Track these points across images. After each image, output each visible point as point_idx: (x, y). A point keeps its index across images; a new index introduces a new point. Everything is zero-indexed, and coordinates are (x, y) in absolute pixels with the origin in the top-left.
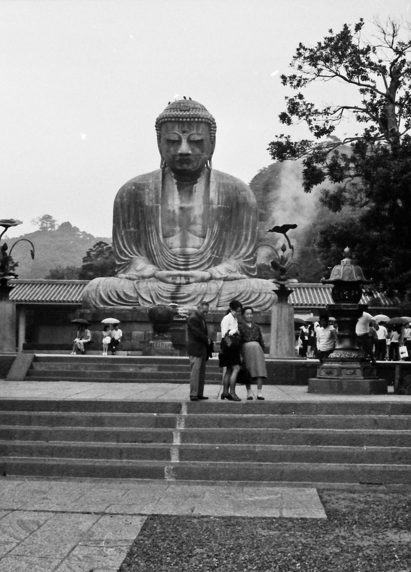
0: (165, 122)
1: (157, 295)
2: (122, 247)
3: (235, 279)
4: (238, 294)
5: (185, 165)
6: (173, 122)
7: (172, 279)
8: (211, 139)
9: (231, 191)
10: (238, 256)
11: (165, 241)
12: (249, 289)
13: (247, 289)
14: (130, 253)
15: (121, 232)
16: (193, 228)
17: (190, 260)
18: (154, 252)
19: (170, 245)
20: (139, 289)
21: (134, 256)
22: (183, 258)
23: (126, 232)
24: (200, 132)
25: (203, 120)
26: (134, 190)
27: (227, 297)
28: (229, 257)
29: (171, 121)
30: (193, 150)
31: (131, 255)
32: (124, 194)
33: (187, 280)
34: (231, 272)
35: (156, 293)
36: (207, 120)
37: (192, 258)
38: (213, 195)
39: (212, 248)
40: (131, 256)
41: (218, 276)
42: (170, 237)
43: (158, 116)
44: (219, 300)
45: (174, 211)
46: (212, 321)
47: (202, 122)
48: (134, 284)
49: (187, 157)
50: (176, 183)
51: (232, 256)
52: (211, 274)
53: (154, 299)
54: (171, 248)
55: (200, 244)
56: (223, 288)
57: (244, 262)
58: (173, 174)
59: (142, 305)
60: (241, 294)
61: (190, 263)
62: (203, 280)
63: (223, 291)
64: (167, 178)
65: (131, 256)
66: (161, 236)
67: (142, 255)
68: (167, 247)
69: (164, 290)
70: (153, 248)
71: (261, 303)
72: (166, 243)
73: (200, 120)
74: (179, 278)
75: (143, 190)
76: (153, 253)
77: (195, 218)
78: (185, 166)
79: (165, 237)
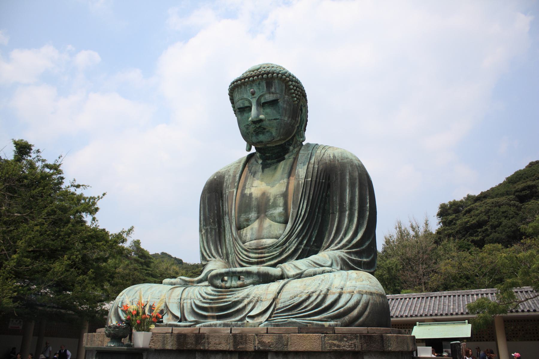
3: (315, 274)
7: (223, 280)
8: (294, 101)
10: (339, 246)
12: (323, 288)
13: (320, 288)
14: (208, 255)
22: (256, 253)
26: (215, 179)
27: (287, 303)
30: (267, 114)
31: (210, 257)
37: (268, 253)
39: (298, 236)
42: (244, 227)
44: (274, 310)
46: (232, 349)
50: (261, 164)
51: (332, 246)
54: (244, 242)
55: (281, 232)
57: (347, 253)
58: (258, 155)
60: (309, 297)
64: (253, 160)
65: (208, 259)
67: (220, 256)
69: (204, 298)
71: (342, 310)
73: (270, 75)
75: (224, 177)
77: (275, 199)
78: (261, 137)
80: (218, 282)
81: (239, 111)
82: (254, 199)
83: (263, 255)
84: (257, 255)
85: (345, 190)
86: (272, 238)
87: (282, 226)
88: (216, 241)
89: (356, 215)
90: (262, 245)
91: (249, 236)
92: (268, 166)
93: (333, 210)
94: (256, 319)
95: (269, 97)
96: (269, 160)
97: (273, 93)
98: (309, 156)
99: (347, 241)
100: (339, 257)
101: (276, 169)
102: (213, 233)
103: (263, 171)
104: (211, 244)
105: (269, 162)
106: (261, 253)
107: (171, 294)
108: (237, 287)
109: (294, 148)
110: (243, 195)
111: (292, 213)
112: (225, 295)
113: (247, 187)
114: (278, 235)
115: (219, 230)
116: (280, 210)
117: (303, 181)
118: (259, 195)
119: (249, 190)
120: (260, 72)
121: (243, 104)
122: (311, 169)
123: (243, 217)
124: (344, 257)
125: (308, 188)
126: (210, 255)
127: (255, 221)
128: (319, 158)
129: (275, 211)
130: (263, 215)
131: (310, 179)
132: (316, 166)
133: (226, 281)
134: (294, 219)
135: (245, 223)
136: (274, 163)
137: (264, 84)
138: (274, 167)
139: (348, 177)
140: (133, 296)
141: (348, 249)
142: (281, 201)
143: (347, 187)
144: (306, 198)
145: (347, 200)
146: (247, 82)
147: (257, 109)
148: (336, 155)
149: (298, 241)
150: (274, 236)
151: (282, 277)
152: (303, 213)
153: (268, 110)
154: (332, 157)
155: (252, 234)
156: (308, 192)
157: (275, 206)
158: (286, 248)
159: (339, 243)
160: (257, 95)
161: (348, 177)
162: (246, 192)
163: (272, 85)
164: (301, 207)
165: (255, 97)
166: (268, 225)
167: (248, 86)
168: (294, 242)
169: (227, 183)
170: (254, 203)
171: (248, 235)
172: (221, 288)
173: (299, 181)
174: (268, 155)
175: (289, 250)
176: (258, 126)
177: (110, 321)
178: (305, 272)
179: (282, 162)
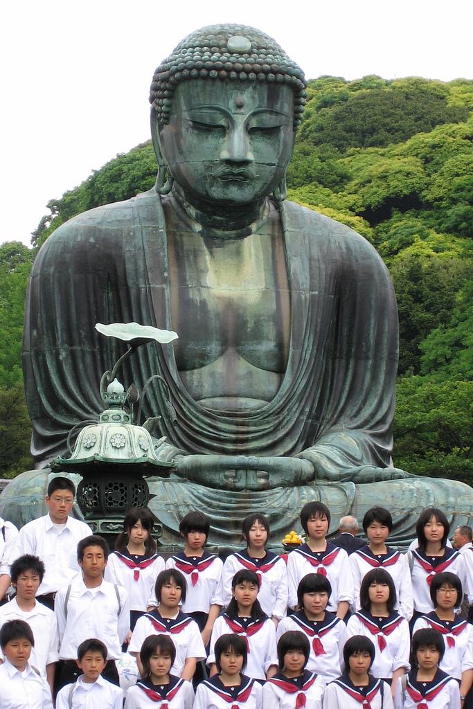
0: (189, 78)
6: (213, 79)
9: (337, 257)
10: (359, 421)
11: (182, 379)
15: (57, 355)
16: (250, 347)
17: (252, 428)
19: (199, 390)
23: (72, 354)
24: (278, 107)
25: (288, 77)
26: (93, 246)
28: (335, 423)
29: (206, 78)
30: (256, 151)
32: (68, 256)
33: (263, 481)
34: (355, 461)
36: (294, 78)
37: (255, 425)
38: (298, 266)
40: (86, 415)
41: (333, 470)
42: (194, 368)
43: (157, 64)
45: (203, 303)
47: (284, 82)
49: (241, 169)
50: (201, 233)
52: (315, 464)
54: (198, 398)
56: (360, 503)
57: (373, 435)
58: (192, 211)
61: (250, 436)
62: (301, 481)
65: (86, 415)
66: (173, 368)
68: (190, 397)
69: (210, 505)
72: (185, 385)
74: (242, 473)
75: (118, 246)
77: (258, 323)
79: (182, 367)
80: (218, 478)
81: (194, 128)
82: (212, 315)
84: (233, 428)
87: (274, 377)
89: (384, 368)
91: (207, 388)
92: (217, 241)
95: (269, 120)
96: (218, 228)
97: (277, 113)
98: (307, 242)
99: (370, 415)
100: (366, 442)
101: (238, 253)
102: (88, 359)
103: (211, 253)
105: (219, 233)
106: (243, 424)
109: (264, 209)
111: (293, 356)
112: (249, 502)
113: (188, 283)
114: (268, 395)
116: (268, 346)
117: (308, 295)
118: (220, 308)
119: (196, 292)
120: (261, 64)
121: (213, 119)
122: (316, 271)
124: (372, 445)
125: (315, 310)
127: (216, 358)
128: (325, 248)
129: (259, 347)
130: (231, 350)
131: (317, 293)
132: (323, 266)
133: (235, 477)
134: (296, 367)
135: (197, 360)
138: (231, 246)
141: (371, 428)
142: (270, 330)
143: (372, 314)
144: (313, 328)
145: (372, 341)
146: (232, 80)
147: (245, 142)
148: (352, 246)
149: (301, 408)
151: (315, 477)
152: (308, 356)
153: (262, 144)
154: (344, 250)
155: (214, 384)
156: (315, 317)
157: (257, 336)
158: (284, 418)
159: (355, 416)
160: (246, 112)
161: (373, 296)
162: (191, 296)
163: (278, 97)
164: (306, 346)
165: (243, 114)
168: (294, 409)
169: (136, 263)
170: (214, 324)
172: (224, 487)
173: (299, 295)
175: (287, 422)
176: (236, 171)
178: (361, 472)
179: (246, 240)
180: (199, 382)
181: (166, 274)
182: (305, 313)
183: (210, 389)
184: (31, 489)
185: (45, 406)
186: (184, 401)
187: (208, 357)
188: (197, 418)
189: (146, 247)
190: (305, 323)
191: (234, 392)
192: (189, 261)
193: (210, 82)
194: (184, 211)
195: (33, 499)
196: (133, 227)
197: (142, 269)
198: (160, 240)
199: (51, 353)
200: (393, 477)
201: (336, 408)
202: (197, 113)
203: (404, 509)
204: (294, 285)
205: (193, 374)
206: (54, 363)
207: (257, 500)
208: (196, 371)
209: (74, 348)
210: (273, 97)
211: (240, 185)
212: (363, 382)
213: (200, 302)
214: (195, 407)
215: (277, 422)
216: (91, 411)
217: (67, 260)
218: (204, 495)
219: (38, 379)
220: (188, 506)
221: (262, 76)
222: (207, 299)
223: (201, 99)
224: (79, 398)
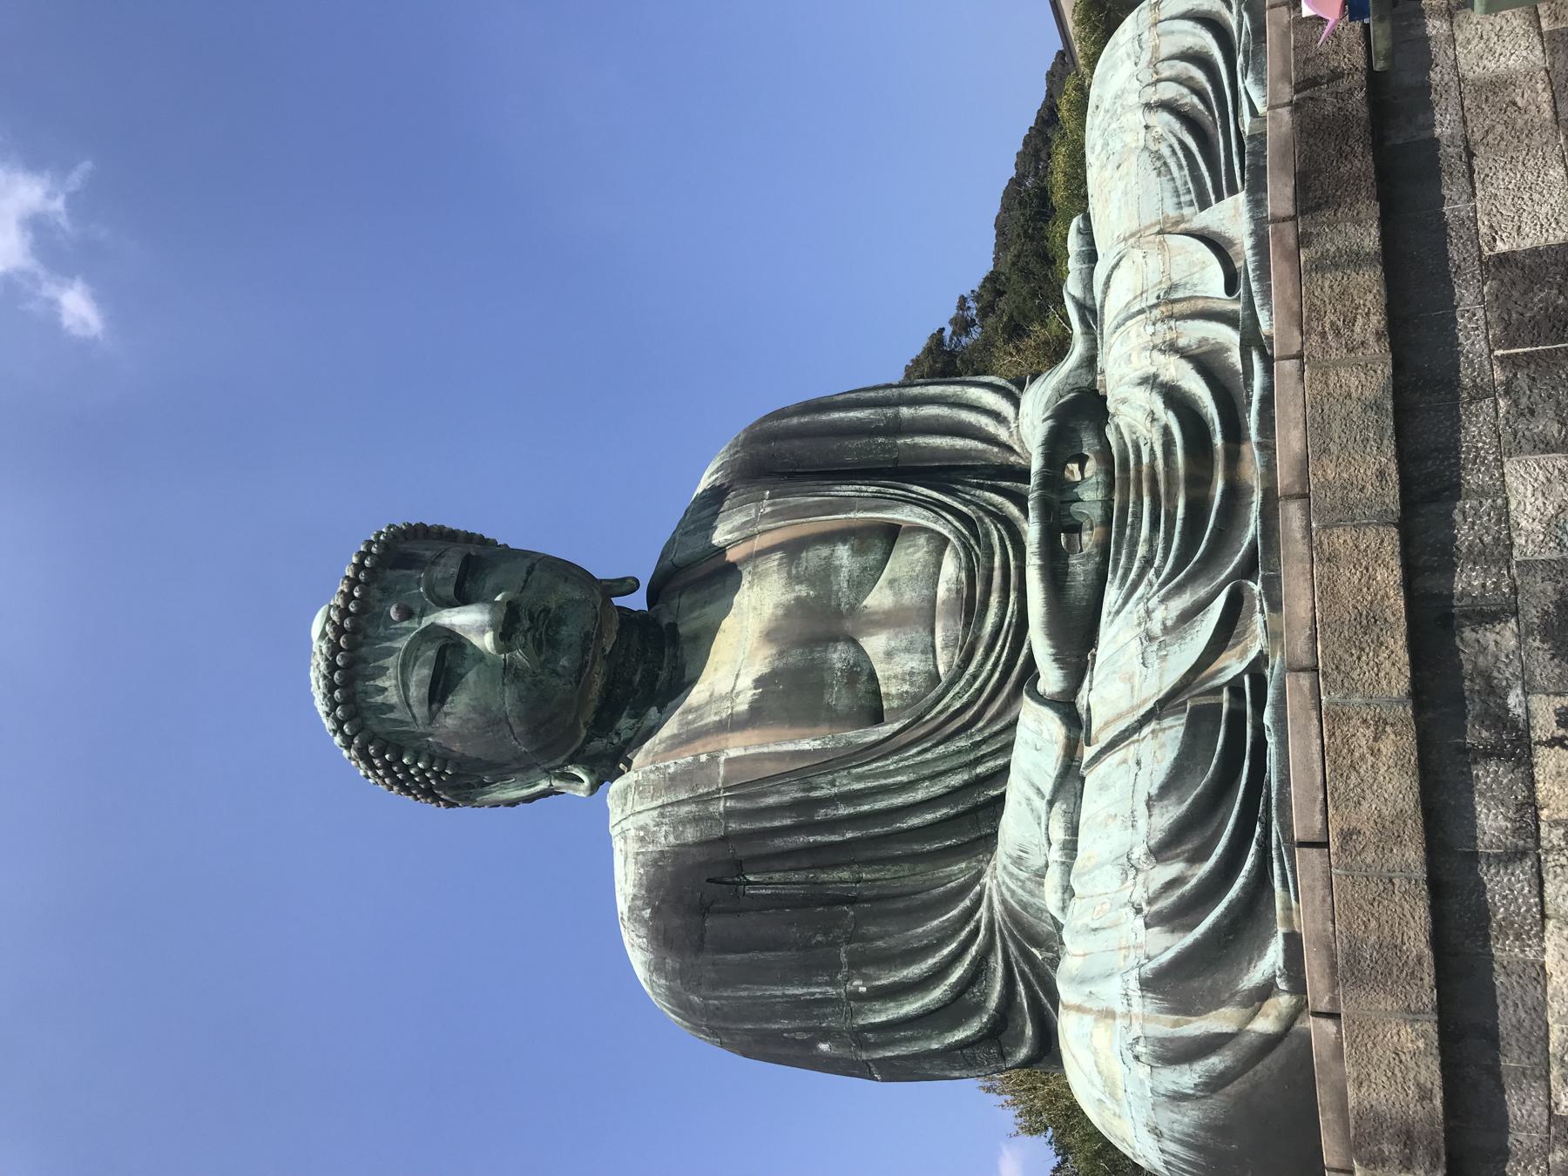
1: (1180, 589)
2: (937, 993)
4: (1166, 117)
5: (565, 631)
10: (1004, 407)
11: (897, 713)
18: (956, 780)
19: (920, 679)
20: (1133, 709)
21: (983, 912)
23: (858, 964)
26: (656, 912)
27: (1181, 175)
28: (1010, 449)
33: (1091, 466)
35: (1162, 601)
39: (952, 493)
42: (876, 693)
45: (759, 682)
48: (1096, 759)
49: (524, 614)
51: (1003, 434)
53: (1202, 592)
54: (934, 678)
55: (922, 540)
59: (1252, 655)
63: (1146, 222)
67: (980, 874)
68: (933, 694)
69: (1148, 562)
70: (937, 788)
72: (908, 706)
76: (967, 786)
79: (877, 717)
81: (443, 702)
82: (780, 664)
83: (997, 575)
84: (994, 600)
85: (832, 424)
86: (938, 565)
88: (908, 912)
90: (959, 591)
91: (914, 663)
93: (886, 461)
94: (1238, 265)
95: (450, 567)
97: (440, 556)
102: (873, 929)
104: (920, 930)
105: (664, 675)
107: (1120, 716)
108: (1110, 473)
110: (756, 716)
111: (866, 510)
112: (1139, 472)
115: (866, 901)
116: (843, 553)
118: (770, 651)
123: (838, 697)
126: (964, 934)
127: (861, 650)
130: (848, 625)
134: (886, 502)
135: (861, 687)
136: (675, 656)
137: (391, 574)
139: (795, 421)
140: (1115, 925)
142: (813, 557)
143: (824, 418)
150: (932, 560)
155: (907, 650)
162: (745, 707)
166: (888, 592)
167: (370, 631)
169: (684, 822)
171: (907, 668)
174: (637, 678)
176: (526, 624)
177: (1265, 1024)
179: (682, 630)
180: (904, 680)
181: (703, 758)
182: (793, 500)
183: (918, 656)
184: (1102, 1061)
185: (968, 1033)
186: (940, 707)
187: (855, 665)
188: (975, 677)
189: (660, 802)
190: (810, 499)
191: (925, 604)
192: (694, 721)
193: (360, 667)
194: (628, 742)
195: (1129, 1056)
196: (632, 833)
197: (693, 807)
198: (652, 776)
199: (858, 1012)
200: (1087, 233)
201: (979, 454)
202: (413, 692)
203: (1147, 127)
204: (748, 532)
205: (888, 694)
206: (877, 1006)
207: (1132, 457)
208: (883, 689)
209: (844, 959)
210: (407, 561)
211: (560, 621)
212: (936, 417)
213: (755, 688)
214: (952, 683)
215: (987, 520)
216: (972, 924)
217: (678, 966)
218: (1122, 584)
219: (915, 1048)
220: (1148, 613)
221: (362, 576)
222: (755, 676)
223: (387, 684)
224: (946, 951)
